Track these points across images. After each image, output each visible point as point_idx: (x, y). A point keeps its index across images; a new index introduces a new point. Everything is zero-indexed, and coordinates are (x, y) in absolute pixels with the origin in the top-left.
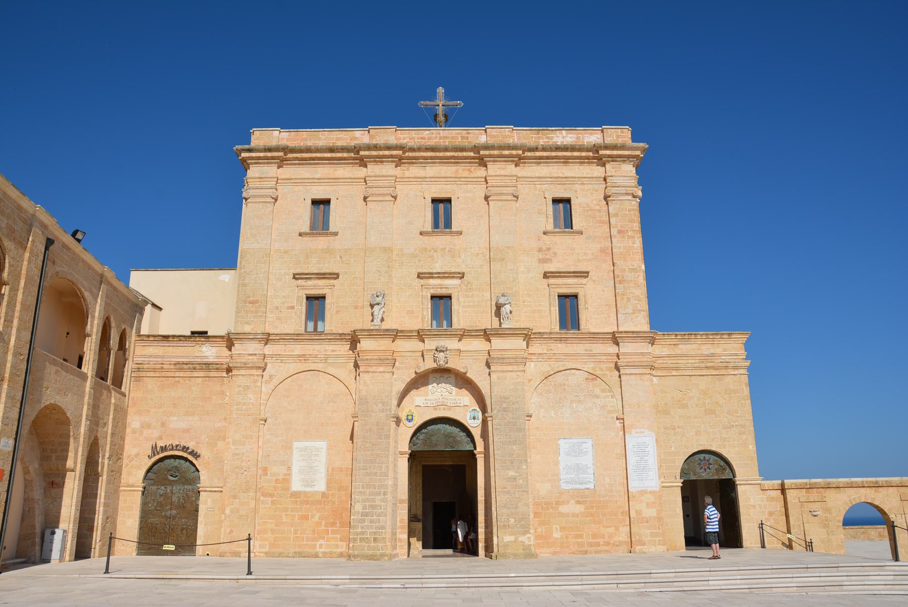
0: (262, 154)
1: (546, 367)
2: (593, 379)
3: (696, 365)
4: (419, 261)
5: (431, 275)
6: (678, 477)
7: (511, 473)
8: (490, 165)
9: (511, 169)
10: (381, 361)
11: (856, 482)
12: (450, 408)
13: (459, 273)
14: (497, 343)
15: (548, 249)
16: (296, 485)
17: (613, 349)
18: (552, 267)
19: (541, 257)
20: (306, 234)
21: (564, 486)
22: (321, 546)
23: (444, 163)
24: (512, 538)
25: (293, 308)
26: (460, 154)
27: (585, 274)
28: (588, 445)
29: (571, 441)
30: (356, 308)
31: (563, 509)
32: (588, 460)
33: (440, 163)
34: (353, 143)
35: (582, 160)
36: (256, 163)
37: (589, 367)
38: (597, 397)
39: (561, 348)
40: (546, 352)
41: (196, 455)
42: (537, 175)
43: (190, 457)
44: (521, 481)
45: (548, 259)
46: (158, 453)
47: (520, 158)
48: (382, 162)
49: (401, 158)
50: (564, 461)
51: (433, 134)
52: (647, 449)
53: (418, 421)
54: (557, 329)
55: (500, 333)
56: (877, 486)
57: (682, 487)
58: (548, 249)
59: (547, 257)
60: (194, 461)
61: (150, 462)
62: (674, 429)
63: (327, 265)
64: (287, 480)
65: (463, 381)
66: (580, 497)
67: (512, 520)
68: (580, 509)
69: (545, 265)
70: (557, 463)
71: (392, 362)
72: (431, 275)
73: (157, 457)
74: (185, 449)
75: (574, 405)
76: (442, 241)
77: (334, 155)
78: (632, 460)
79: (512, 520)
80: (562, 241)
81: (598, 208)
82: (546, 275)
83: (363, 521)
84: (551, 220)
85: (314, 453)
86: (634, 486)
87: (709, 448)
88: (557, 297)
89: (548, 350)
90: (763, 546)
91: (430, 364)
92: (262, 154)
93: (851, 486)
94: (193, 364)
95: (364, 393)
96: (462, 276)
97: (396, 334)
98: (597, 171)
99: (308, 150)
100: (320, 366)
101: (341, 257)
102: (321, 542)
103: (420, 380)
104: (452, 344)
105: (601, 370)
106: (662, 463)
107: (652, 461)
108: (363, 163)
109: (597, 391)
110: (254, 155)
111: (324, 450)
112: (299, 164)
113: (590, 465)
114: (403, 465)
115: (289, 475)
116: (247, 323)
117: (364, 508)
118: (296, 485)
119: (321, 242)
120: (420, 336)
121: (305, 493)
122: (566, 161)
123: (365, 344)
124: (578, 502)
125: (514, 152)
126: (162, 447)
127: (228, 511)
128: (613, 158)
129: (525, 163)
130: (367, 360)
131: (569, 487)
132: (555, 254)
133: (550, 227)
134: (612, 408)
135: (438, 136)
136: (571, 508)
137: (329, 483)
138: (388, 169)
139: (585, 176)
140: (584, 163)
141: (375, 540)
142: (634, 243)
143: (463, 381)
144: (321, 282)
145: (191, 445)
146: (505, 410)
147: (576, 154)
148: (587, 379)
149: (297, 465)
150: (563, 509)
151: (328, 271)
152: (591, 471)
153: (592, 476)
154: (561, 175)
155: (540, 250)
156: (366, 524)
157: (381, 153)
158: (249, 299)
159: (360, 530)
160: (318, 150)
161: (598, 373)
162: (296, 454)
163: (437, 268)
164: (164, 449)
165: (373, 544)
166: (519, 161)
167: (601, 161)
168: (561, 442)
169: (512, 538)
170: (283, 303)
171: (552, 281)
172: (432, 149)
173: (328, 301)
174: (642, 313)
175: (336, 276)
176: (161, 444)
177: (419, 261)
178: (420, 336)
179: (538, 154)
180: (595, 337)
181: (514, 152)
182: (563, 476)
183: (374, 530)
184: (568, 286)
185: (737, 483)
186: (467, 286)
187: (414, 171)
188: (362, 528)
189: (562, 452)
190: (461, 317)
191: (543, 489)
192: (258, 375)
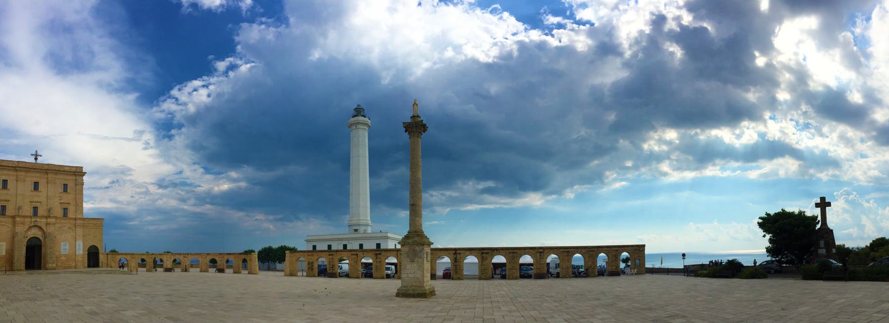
1: (59, 225)
5: (33, 202)
8: (49, 175)
9: (54, 176)
10: (22, 223)
14: (49, 220)
17: (74, 222)
18: (62, 201)
21: (62, 253)
27: (69, 203)
28: (68, 244)
31: (61, 258)
34: (14, 166)
35: (71, 175)
37: (69, 226)
39: (63, 221)
49: (27, 171)
50: (62, 247)
53: (29, 238)
54: (62, 216)
55: (49, 217)
65: (40, 228)
66: (65, 256)
68: (65, 258)
70: (60, 248)
71: (23, 223)
72: (33, 202)
76: (36, 193)
78: (77, 247)
80: (64, 195)
82: (61, 203)
84: (62, 190)
86: (77, 253)
91: (33, 224)
96: (40, 202)
97: (25, 217)
98: (74, 178)
100: (5, 224)
103: (30, 227)
104: (38, 220)
106: (84, 248)
107: (82, 248)
108: (17, 171)
114: (25, 248)
120: (31, 217)
122: (67, 175)
123: (18, 219)
128: (79, 175)
133: (62, 191)
136: (63, 258)
143: (40, 228)
144: (5, 202)
150: (61, 258)
163: (35, 199)
166: (56, 174)
167: (76, 175)
168: (62, 243)
171: (62, 205)
173: (7, 207)
175: (9, 201)
178: (31, 217)
180: (71, 219)
182: (62, 251)
184: (65, 206)
187: (30, 174)
190: (41, 212)
191: (57, 254)
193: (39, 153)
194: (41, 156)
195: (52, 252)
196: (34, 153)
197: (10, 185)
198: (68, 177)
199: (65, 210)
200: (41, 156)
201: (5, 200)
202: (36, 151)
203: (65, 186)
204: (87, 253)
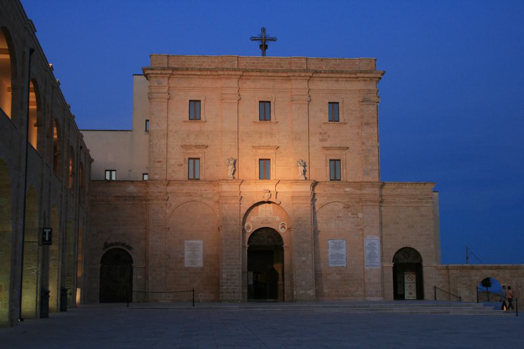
0: (159, 72)
2: (348, 208)
3: (405, 201)
4: (253, 139)
6: (392, 262)
7: (304, 258)
11: (487, 266)
12: (270, 223)
13: (275, 147)
15: (326, 133)
16: (187, 264)
18: (327, 144)
19: (321, 138)
20: (187, 121)
21: (331, 265)
22: (201, 296)
23: (267, 79)
24: (303, 292)
25: (182, 165)
26: (276, 74)
29: (335, 241)
30: (217, 166)
32: (343, 251)
33: (264, 79)
35: (348, 79)
36: (155, 77)
38: (350, 217)
40: (322, 192)
41: (130, 248)
42: (320, 88)
43: (127, 249)
44: (308, 263)
45: (324, 139)
46: (108, 247)
47: (311, 77)
48: (230, 78)
51: (259, 60)
52: (375, 246)
56: (498, 268)
57: (393, 267)
58: (326, 133)
59: (325, 138)
60: (129, 252)
61: (104, 252)
62: (391, 235)
63: (200, 140)
64: (182, 261)
67: (304, 283)
69: (324, 143)
72: (259, 148)
73: (108, 249)
74: (123, 245)
75: (337, 222)
77: (202, 73)
78: (367, 252)
79: (304, 283)
81: (354, 108)
83: (228, 283)
85: (196, 247)
87: (409, 246)
88: (329, 161)
89: (323, 191)
90: (436, 299)
92: (159, 72)
93: (485, 268)
94: (125, 197)
95: (225, 215)
99: (187, 69)
101: (208, 136)
102: (202, 294)
105: (352, 202)
109: (350, 214)
110: (154, 72)
111: (202, 245)
112: (181, 78)
113: (345, 254)
115: (183, 258)
116: (156, 174)
117: (227, 276)
118: (187, 264)
119: (195, 126)
121: (192, 268)
124: (338, 274)
125: (308, 74)
126: (110, 244)
127: (150, 279)
129: (313, 80)
130: (226, 196)
131: (334, 265)
132: (329, 136)
134: (357, 224)
135: (263, 62)
137: (205, 261)
138: (234, 83)
139: (348, 89)
140: (348, 81)
141: (234, 292)
142: (374, 130)
144: (197, 151)
145: (127, 243)
146: (300, 225)
147: (343, 76)
148: (344, 207)
149: (187, 253)
151: (200, 144)
152: (345, 257)
153: (345, 260)
154: (334, 88)
155: (321, 134)
156: (229, 284)
157: (230, 73)
158: (156, 160)
159: (226, 287)
160: (192, 69)
161: (351, 204)
162: (186, 246)
164: (111, 245)
165: (232, 295)
169: (303, 292)
170: (176, 162)
171: (328, 152)
172: (260, 71)
174: (376, 171)
176: (109, 242)
177: (253, 139)
179: (321, 75)
180: (349, 184)
181: (308, 74)
183: (233, 287)
184: (335, 155)
185: (423, 265)
186: (279, 154)
188: (227, 286)
189: (330, 246)
192: (164, 204)
193: (270, 33)
194: (273, 40)
195: (305, 261)
196: (257, 33)
197: (207, 111)
198: (343, 85)
199: (335, 164)
200: (273, 40)
201: (197, 147)
202: (264, 30)
203: (334, 106)
204: (392, 265)
